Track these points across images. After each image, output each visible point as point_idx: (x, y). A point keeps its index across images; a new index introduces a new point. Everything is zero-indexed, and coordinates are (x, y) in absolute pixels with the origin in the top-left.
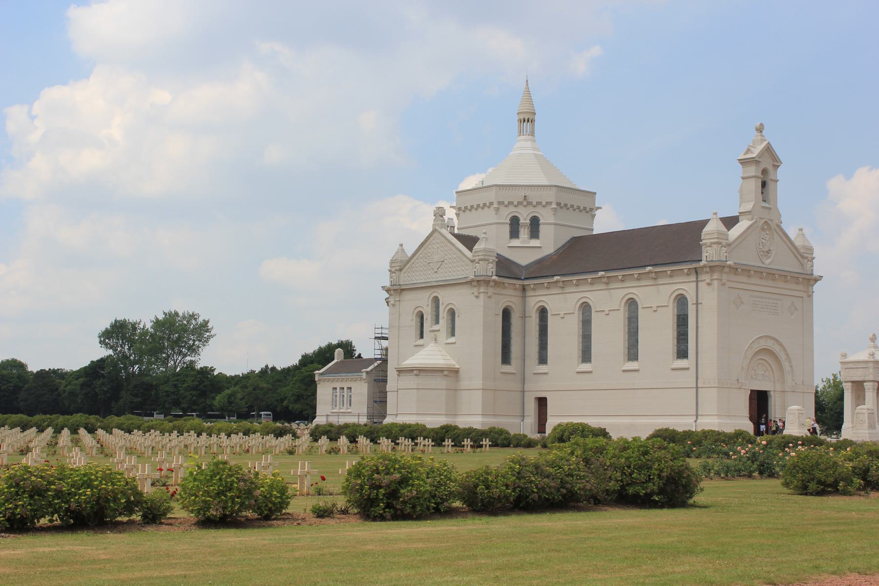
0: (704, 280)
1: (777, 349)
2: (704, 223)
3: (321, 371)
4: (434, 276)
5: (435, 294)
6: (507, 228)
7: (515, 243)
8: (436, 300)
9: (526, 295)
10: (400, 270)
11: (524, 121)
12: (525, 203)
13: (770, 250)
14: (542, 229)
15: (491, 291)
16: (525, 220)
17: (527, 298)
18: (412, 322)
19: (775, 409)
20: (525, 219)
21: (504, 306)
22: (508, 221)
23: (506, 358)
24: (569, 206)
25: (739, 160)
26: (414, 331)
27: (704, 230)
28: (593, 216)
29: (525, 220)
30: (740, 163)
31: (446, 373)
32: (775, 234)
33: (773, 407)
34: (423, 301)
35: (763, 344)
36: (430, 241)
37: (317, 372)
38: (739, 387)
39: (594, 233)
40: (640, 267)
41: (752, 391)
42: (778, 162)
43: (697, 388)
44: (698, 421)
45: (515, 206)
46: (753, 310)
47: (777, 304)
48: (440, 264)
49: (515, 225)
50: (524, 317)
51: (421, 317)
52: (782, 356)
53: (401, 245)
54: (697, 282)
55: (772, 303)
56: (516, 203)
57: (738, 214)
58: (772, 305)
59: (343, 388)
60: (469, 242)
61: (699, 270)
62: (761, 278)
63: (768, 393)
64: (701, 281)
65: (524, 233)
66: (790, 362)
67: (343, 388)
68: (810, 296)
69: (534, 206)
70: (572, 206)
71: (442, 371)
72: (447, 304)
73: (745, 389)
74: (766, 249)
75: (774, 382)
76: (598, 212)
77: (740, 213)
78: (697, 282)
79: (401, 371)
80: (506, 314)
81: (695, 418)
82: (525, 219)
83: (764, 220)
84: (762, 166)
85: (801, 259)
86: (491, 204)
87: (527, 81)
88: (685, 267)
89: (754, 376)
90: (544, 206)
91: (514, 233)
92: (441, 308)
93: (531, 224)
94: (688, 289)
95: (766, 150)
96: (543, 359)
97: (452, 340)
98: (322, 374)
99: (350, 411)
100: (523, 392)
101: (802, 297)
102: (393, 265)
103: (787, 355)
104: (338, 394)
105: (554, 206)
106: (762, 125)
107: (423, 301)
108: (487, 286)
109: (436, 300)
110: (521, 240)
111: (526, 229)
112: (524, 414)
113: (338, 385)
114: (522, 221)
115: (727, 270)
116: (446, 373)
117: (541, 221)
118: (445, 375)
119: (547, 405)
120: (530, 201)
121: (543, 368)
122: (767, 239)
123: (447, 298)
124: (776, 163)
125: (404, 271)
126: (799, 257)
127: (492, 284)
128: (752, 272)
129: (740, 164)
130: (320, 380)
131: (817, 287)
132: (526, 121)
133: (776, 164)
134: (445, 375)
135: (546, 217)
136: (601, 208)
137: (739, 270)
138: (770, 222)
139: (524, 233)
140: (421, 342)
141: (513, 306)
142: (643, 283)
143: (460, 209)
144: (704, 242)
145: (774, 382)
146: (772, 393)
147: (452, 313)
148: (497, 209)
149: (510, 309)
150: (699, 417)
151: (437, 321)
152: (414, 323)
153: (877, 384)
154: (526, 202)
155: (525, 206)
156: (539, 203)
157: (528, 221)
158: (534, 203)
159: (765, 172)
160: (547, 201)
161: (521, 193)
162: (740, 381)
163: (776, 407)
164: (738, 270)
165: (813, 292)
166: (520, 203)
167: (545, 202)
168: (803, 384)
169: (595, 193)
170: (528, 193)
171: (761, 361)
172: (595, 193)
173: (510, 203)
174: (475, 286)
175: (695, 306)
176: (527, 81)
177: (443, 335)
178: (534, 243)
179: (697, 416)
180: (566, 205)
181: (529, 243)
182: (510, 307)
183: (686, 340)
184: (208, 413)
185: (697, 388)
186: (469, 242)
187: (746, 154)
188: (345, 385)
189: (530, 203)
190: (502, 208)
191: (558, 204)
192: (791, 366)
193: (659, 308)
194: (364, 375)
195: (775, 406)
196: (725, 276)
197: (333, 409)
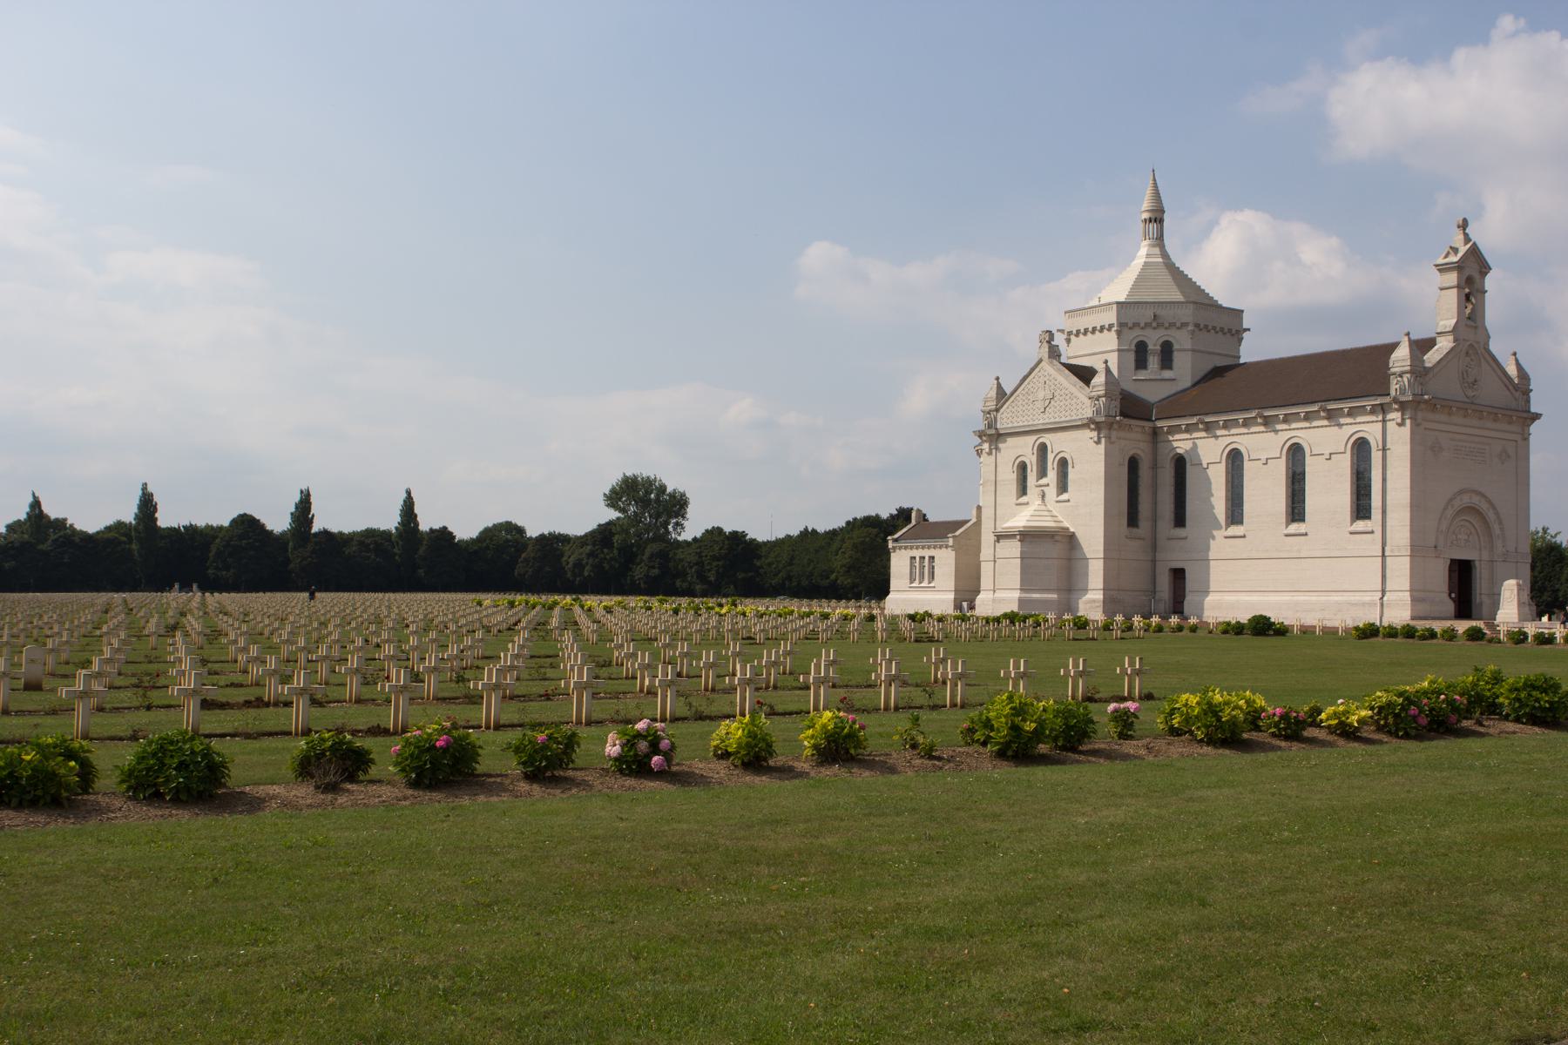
0: (1393, 420)
1: (1484, 506)
2: (1392, 347)
3: (896, 536)
5: (1041, 440)
6: (1131, 357)
7: (1142, 375)
8: (1043, 450)
9: (1158, 440)
10: (997, 410)
11: (1150, 221)
12: (1154, 324)
13: (1476, 381)
14: (1177, 357)
15: (1114, 434)
16: (1154, 345)
17: (1160, 445)
18: (1009, 476)
19: (1481, 583)
20: (1155, 345)
21: (1131, 453)
22: (1133, 347)
23: (1133, 520)
24: (1210, 327)
25: (1436, 266)
26: (1013, 487)
27: (1393, 356)
28: (1240, 340)
29: (1154, 345)
30: (1438, 270)
31: (1057, 538)
32: (1482, 360)
33: (1478, 581)
34: (1023, 448)
35: (1466, 500)
36: (1033, 374)
37: (889, 538)
39: (1242, 361)
41: (1453, 561)
42: (1485, 268)
43: (1383, 555)
44: (1385, 598)
45: (1142, 328)
47: (1484, 449)
48: (1048, 402)
49: (1140, 355)
50: (1155, 466)
51: (1023, 468)
52: (1491, 515)
53: (998, 379)
54: (1384, 421)
56: (1142, 325)
57: (1434, 335)
59: (924, 558)
60: (1084, 374)
61: (1385, 407)
62: (1465, 416)
63: (1472, 563)
64: (1390, 420)
65: (1153, 362)
66: (1500, 523)
67: (924, 558)
68: (1526, 438)
69: (1166, 328)
70: (1214, 328)
71: (1053, 536)
72: (1057, 452)
74: (1471, 380)
75: (1480, 550)
76: (1245, 335)
77: (1438, 333)
78: (1384, 421)
79: (999, 537)
80: (1133, 464)
81: (1380, 594)
82: (1155, 345)
83: (1468, 343)
84: (1467, 273)
85: (1514, 392)
86: (1111, 327)
87: (1154, 171)
88: (1368, 403)
89: (1455, 542)
90: (1178, 328)
91: (1141, 363)
92: (1050, 457)
93: (1162, 351)
94: (1370, 428)
95: (1472, 252)
96: (1180, 520)
97: (1064, 497)
98: (896, 540)
99: (932, 585)
100: (1154, 561)
101: (1516, 441)
102: (987, 404)
103: (1497, 514)
104: (917, 564)
105: (1190, 328)
106: (1465, 221)
108: (1110, 429)
109: (1043, 450)
110: (1149, 371)
111: (1156, 358)
112: (1155, 588)
113: (917, 553)
114: (1150, 347)
115: (1423, 406)
116: (1057, 538)
117: (1176, 347)
119: (1184, 578)
121: (1180, 532)
123: (1058, 444)
124: (1484, 268)
125: (1002, 411)
126: (1511, 387)
127: (1115, 426)
128: (1454, 409)
129: (1437, 272)
130: (894, 548)
131: (1535, 428)
132: (1153, 221)
133: (1484, 270)
135: (1182, 340)
136: (1249, 330)
137: (1438, 406)
138: (1476, 345)
139: (1153, 362)
140: (1024, 499)
141: (1139, 452)
142: (1315, 423)
143: (1070, 333)
144: (1393, 370)
145: (1480, 550)
146: (1477, 564)
147: (1063, 464)
149: (1138, 457)
150: (1388, 594)
151: (1042, 473)
152: (1014, 476)
154: (1156, 322)
155: (1155, 328)
156: (1172, 325)
157: (1159, 348)
159: (1469, 281)
160: (1183, 321)
161: (1148, 314)
162: (1439, 548)
163: (1483, 581)
165: (1530, 434)
166: (1147, 325)
168: (1516, 552)
169: (1242, 311)
170: (1160, 312)
171: (1467, 524)
172: (1242, 311)
173: (1136, 325)
174: (1094, 430)
175: (1381, 452)
177: (1051, 492)
178: (1167, 374)
179: (1383, 592)
180: (1206, 326)
181: (1160, 375)
182: (1138, 455)
183: (1369, 495)
184: (1127, 658)
185: (1383, 555)
186: (1084, 374)
187: (1446, 257)
188: (927, 553)
189: (1160, 325)
190: (1125, 330)
191: (1197, 325)
192: (1502, 529)
194: (951, 542)
195: (1481, 578)
196: (1420, 415)
197: (911, 583)
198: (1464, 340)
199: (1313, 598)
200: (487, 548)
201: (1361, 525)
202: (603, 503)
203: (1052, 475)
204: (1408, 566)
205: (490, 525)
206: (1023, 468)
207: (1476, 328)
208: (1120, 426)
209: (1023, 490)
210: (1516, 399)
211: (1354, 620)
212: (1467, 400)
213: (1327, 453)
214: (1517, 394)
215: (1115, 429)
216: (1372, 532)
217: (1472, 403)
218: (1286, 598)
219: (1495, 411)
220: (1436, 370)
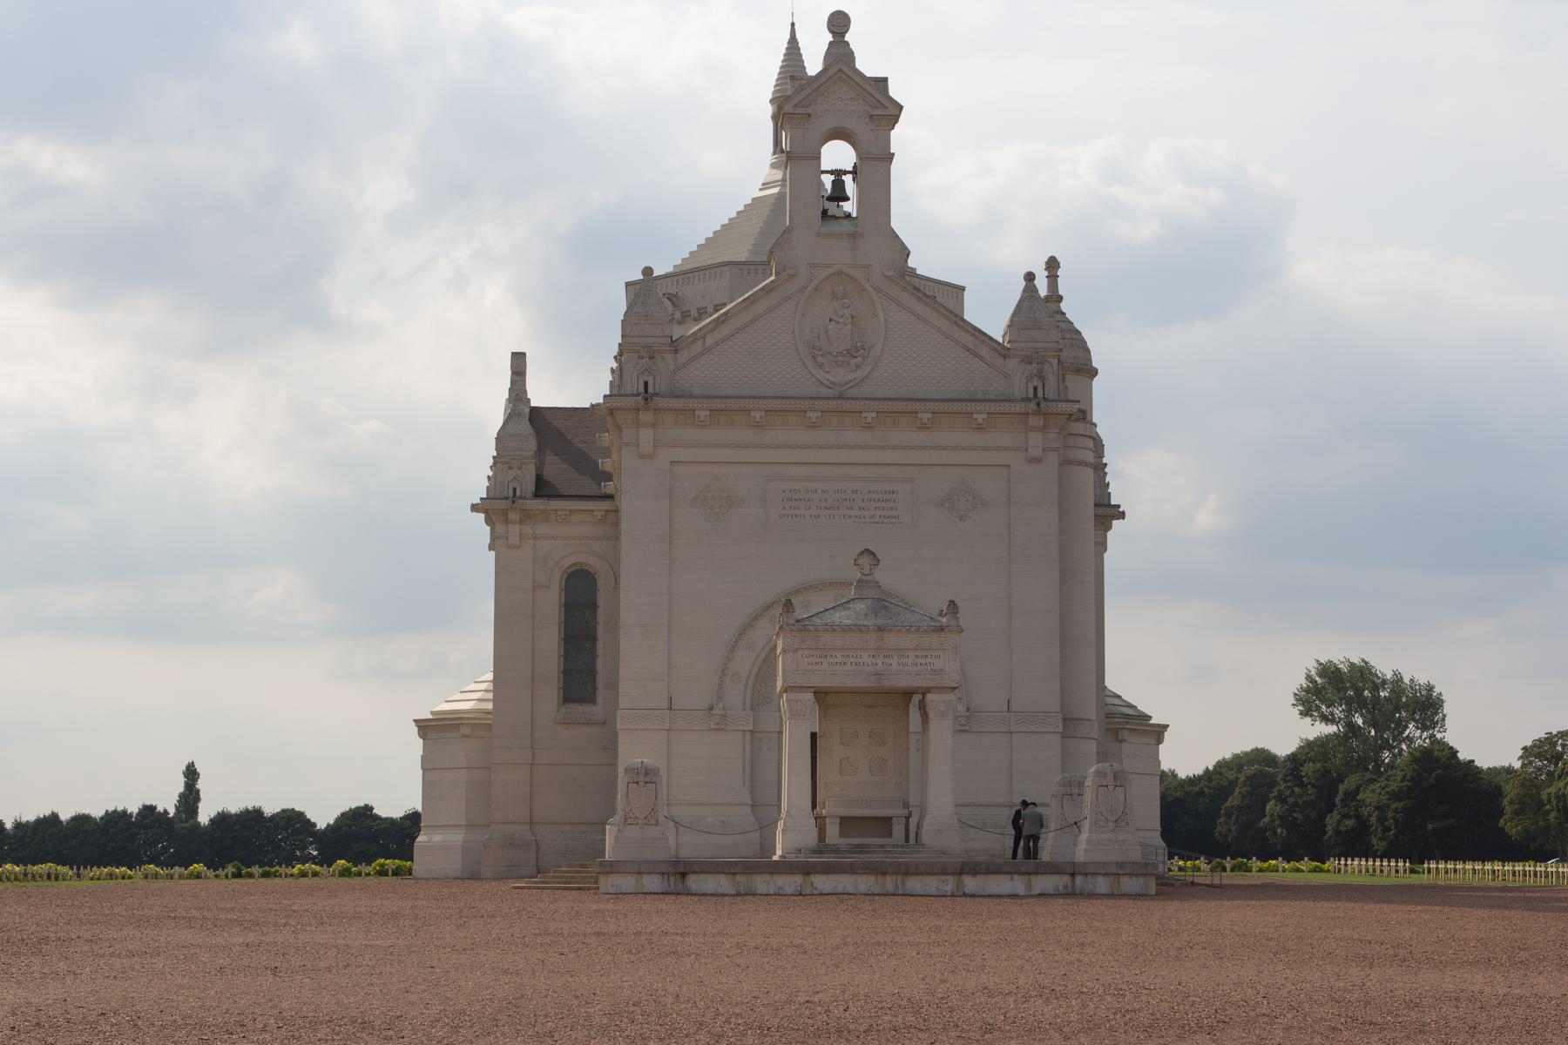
12: (678, 315)
13: (851, 353)
15: (514, 530)
31: (465, 730)
38: (712, 727)
46: (780, 516)
55: (869, 492)
58: (873, 496)
73: (744, 731)
87: (793, 25)
108: (507, 522)
116: (465, 730)
118: (464, 736)
120: (685, 309)
122: (841, 320)
126: (984, 351)
134: (464, 736)
137: (702, 414)
153: (810, 696)
158: (694, 313)
164: (697, 413)
167: (712, 306)
176: (793, 25)
189: (685, 316)
198: (812, 266)
200: (1201, 794)
202: (1296, 711)
205: (1228, 756)
207: (853, 236)
208: (526, 517)
210: (1006, 376)
212: (824, 392)
214: (1012, 363)
215: (515, 523)
217: (841, 397)
219: (900, 406)
220: (710, 340)
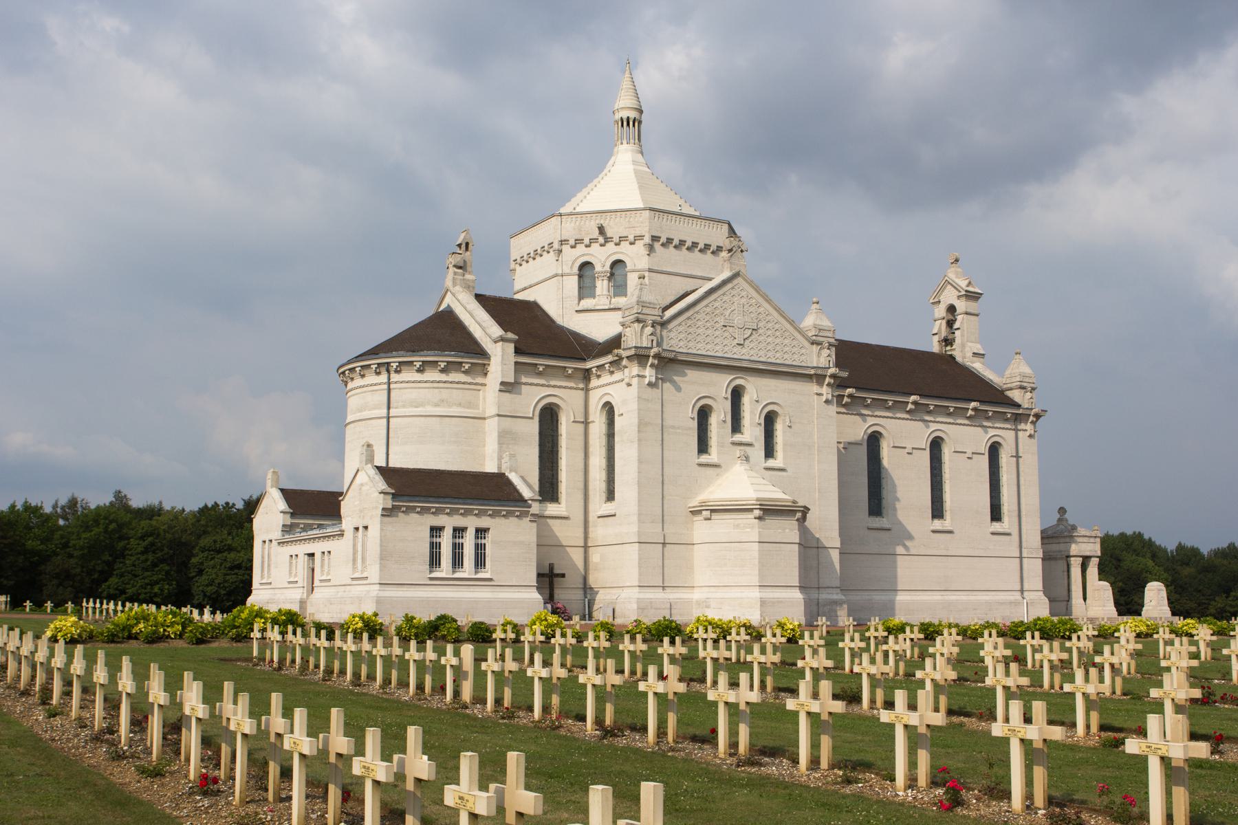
4: (735, 350)
8: (737, 395)
34: (717, 387)
40: (889, 391)
43: (1021, 558)
51: (704, 414)
107: (717, 387)
109: (737, 395)
113: (449, 522)
148: (651, 248)
151: (736, 427)
193: (974, 455)
199: (963, 597)
201: (997, 526)
203: (752, 430)
204: (1040, 567)
206: (704, 414)
209: (703, 447)
211: (1003, 619)
213: (969, 451)
216: (1009, 534)
218: (937, 597)
